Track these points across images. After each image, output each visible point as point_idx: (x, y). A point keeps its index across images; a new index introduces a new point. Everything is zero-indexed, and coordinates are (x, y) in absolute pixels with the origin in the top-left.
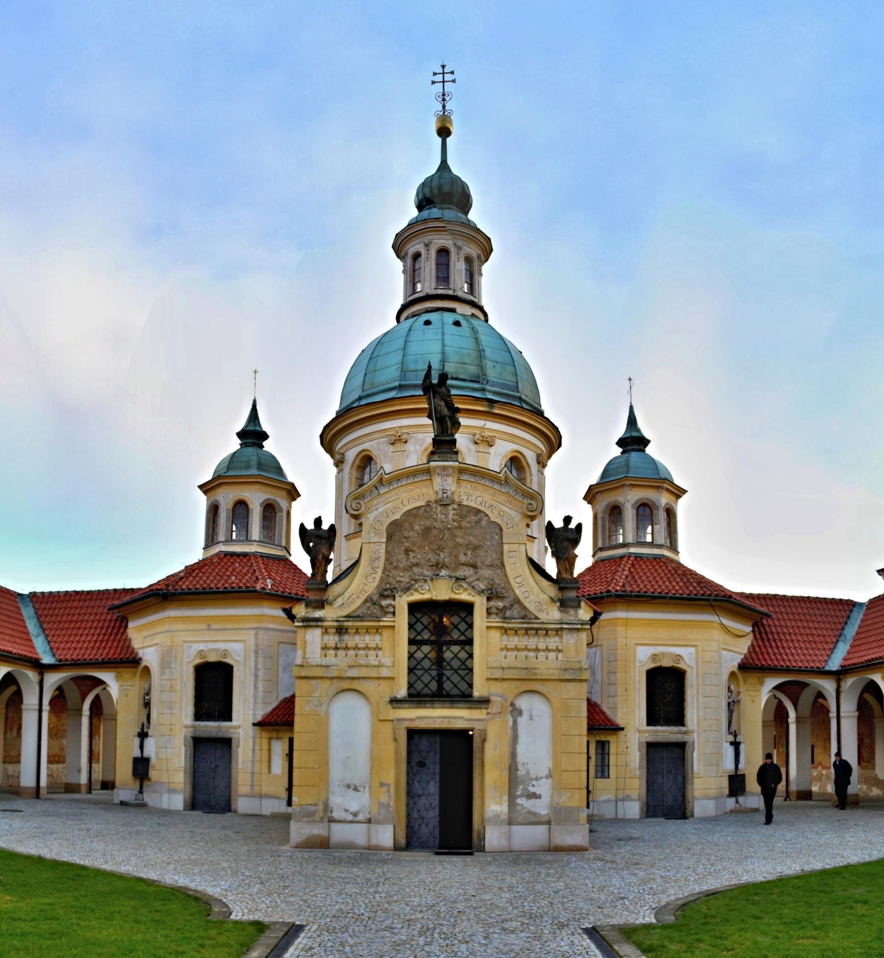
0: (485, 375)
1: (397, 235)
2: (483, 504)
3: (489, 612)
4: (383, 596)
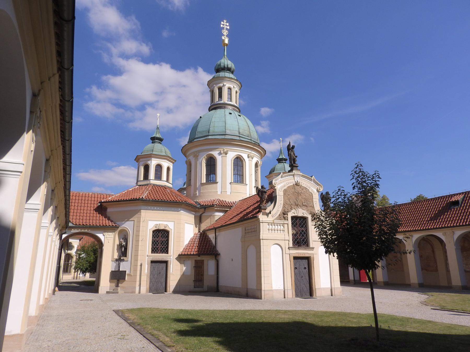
4: (284, 214)
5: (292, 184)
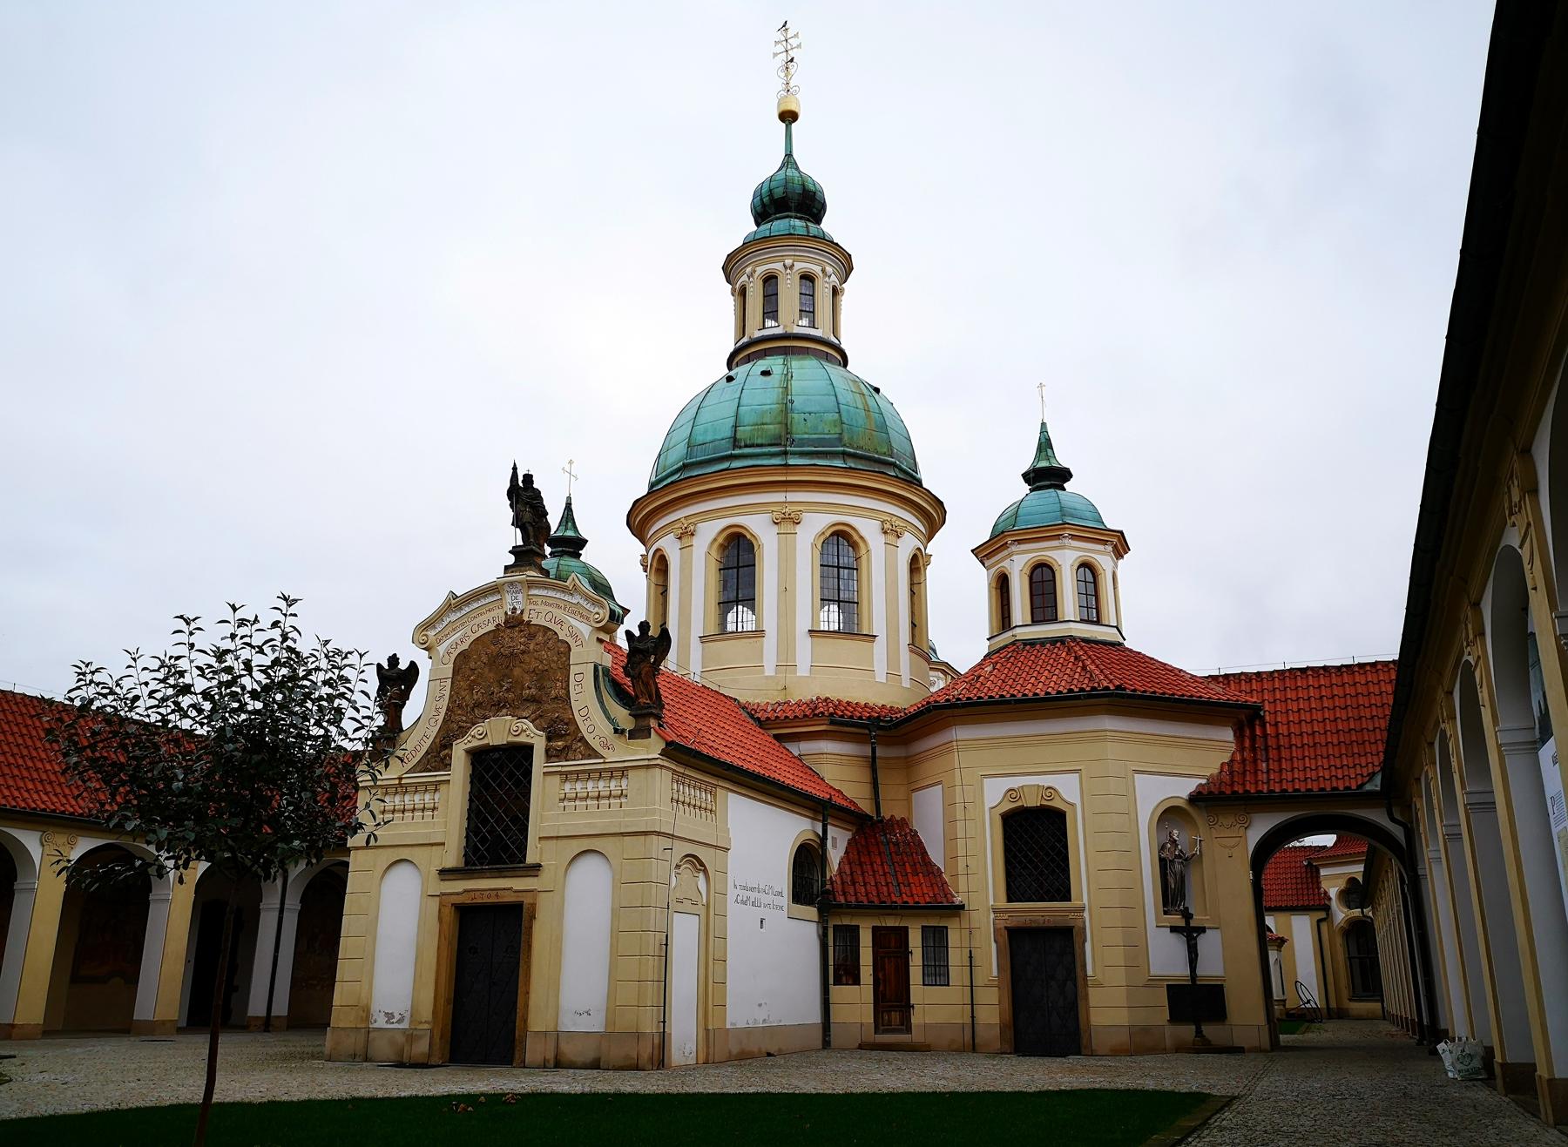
0: (790, 433)
1: (723, 268)
2: (553, 621)
3: (550, 755)
5: (491, 627)
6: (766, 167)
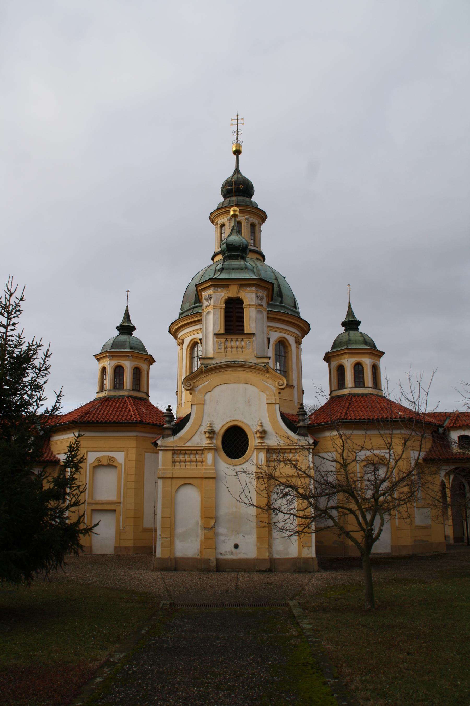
6: (228, 173)
